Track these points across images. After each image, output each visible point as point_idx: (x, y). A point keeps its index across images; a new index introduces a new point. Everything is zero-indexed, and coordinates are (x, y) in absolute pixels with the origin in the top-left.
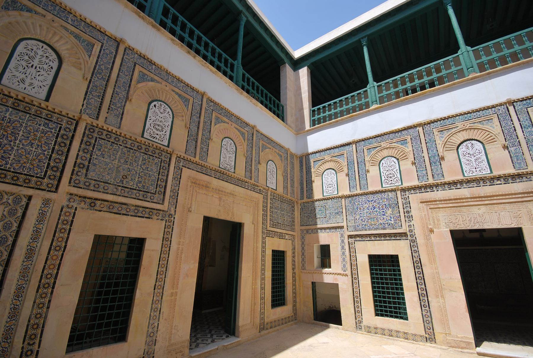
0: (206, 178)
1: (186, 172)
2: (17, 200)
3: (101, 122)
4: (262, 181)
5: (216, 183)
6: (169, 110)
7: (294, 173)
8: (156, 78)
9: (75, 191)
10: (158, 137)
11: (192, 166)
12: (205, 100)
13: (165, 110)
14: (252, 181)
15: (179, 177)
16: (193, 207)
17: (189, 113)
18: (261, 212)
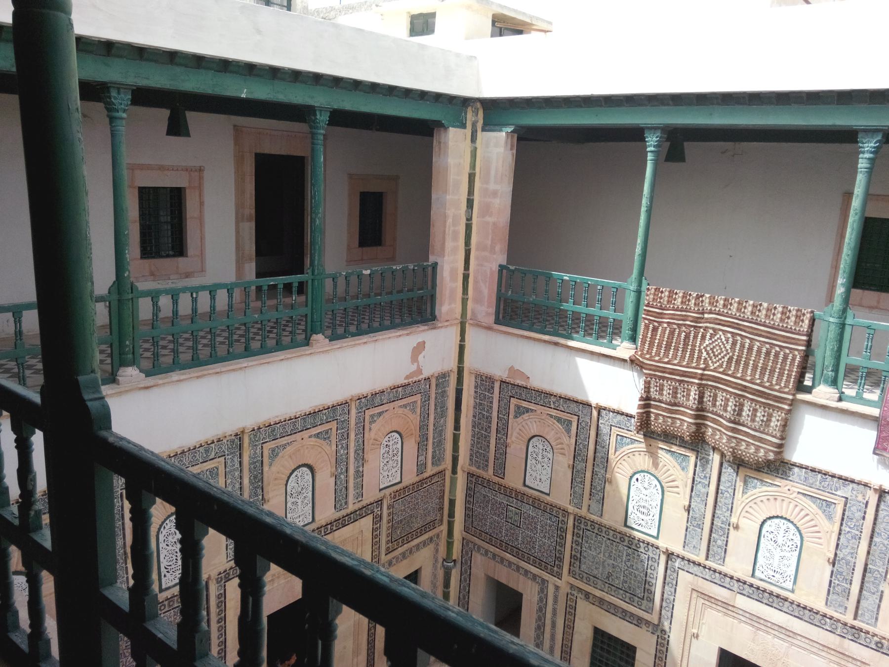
1: (684, 578)
2: (543, 581)
3: (583, 512)
5: (742, 602)
6: (656, 482)
9: (572, 581)
10: (643, 523)
11: (695, 569)
13: (650, 484)
15: (674, 582)
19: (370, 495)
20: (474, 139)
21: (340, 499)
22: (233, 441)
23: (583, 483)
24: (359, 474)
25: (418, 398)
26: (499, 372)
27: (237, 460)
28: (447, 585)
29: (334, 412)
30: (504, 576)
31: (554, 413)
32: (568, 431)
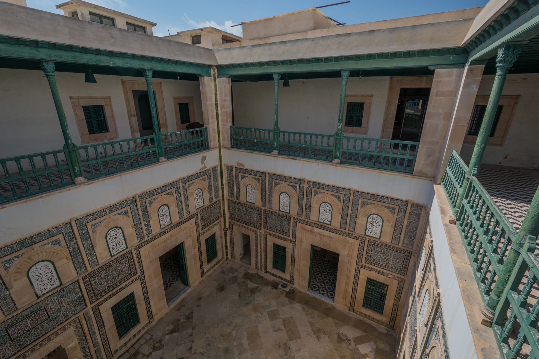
0: (310, 228)
4: (359, 231)
5: (316, 230)
7: (418, 224)
8: (280, 182)
11: (301, 222)
12: (306, 184)
14: (347, 231)
16: (304, 240)
17: (298, 194)
18: (356, 252)
19: (192, 211)
20: (215, 81)
21: (181, 214)
22: (132, 200)
23: (265, 198)
24: (187, 205)
25: (206, 176)
26: (235, 165)
27: (135, 206)
28: (226, 236)
29: (174, 185)
30: (244, 231)
31: (254, 177)
32: (259, 182)
